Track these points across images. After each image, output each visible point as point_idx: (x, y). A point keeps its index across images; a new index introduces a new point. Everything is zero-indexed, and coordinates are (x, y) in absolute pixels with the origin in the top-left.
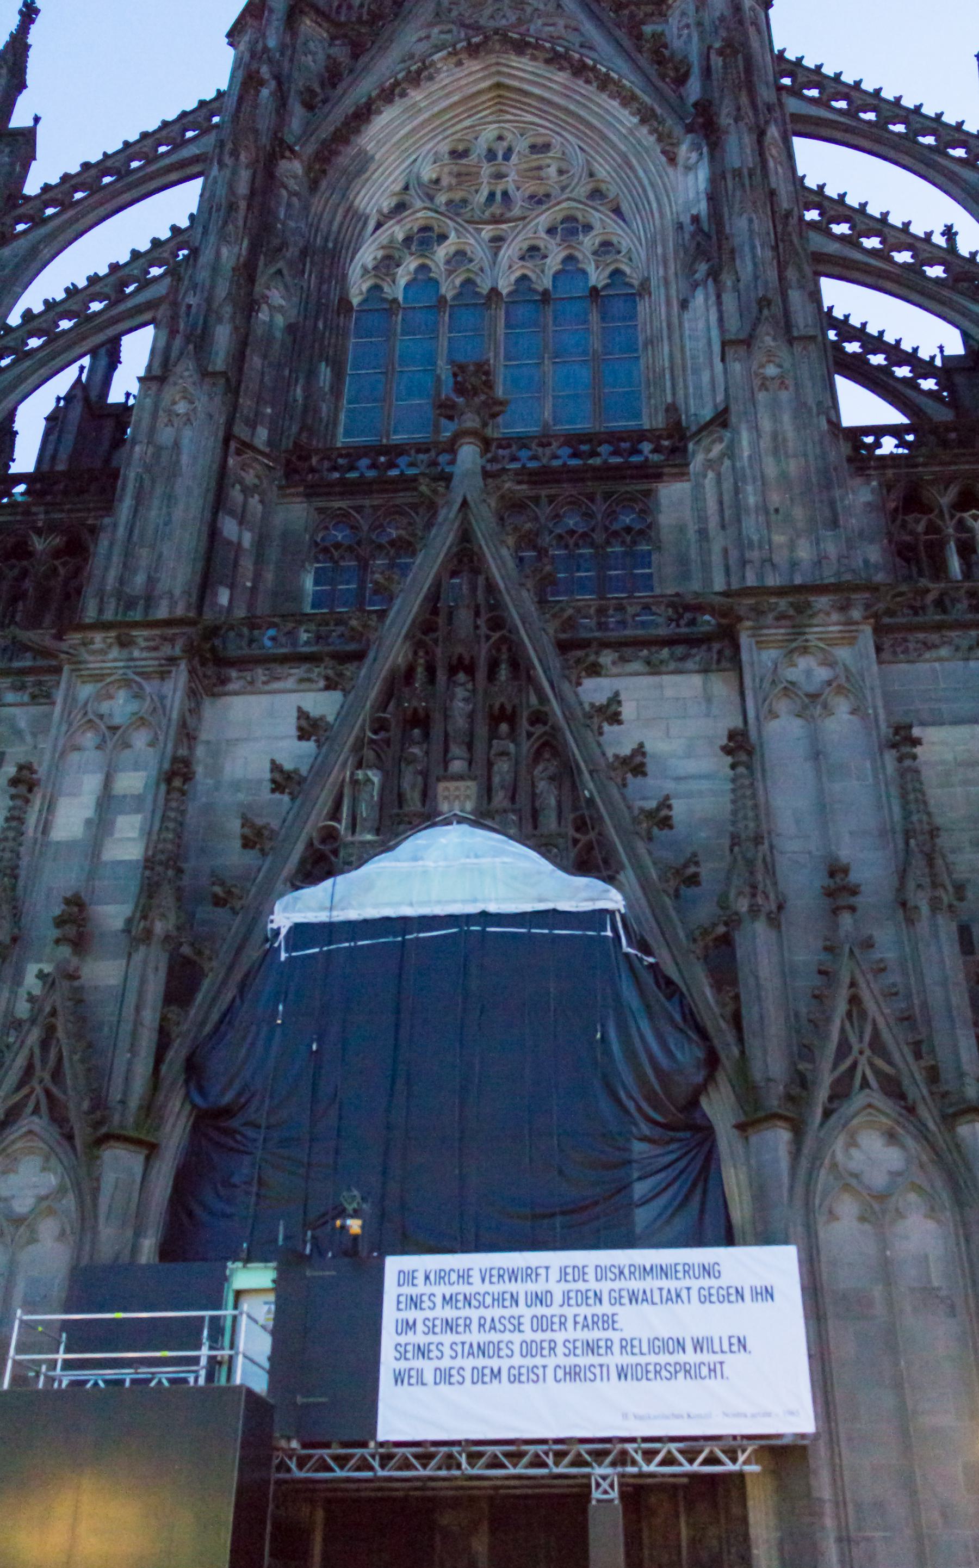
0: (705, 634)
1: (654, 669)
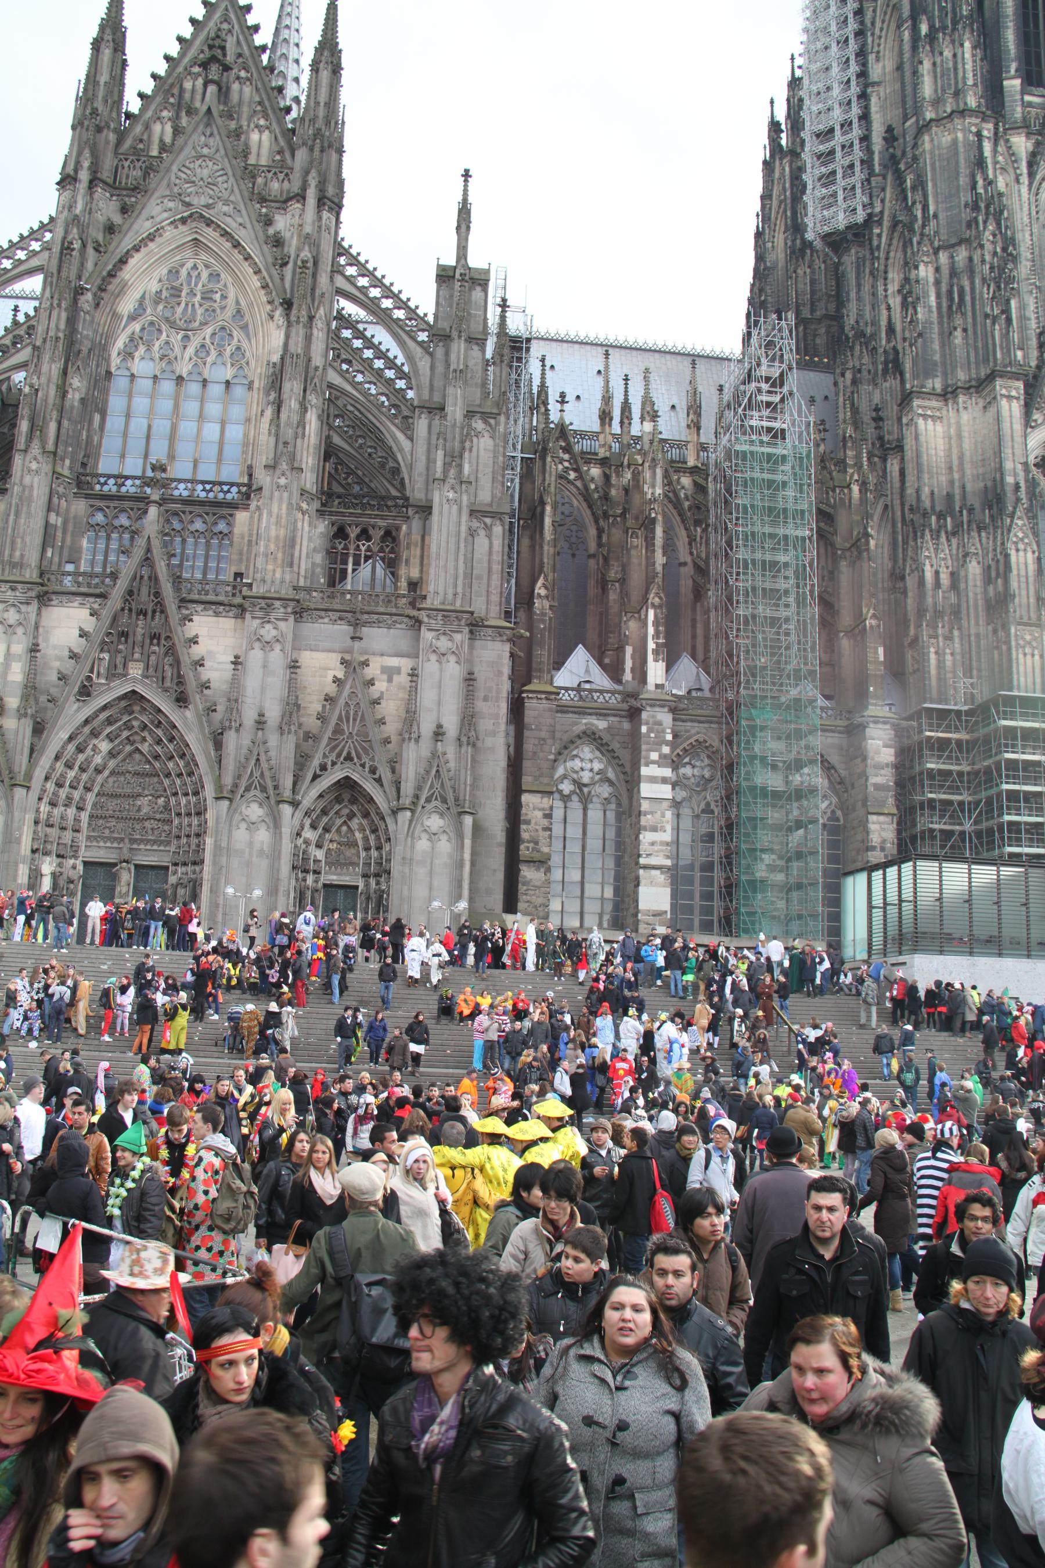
0: (239, 601)
1: (217, 614)
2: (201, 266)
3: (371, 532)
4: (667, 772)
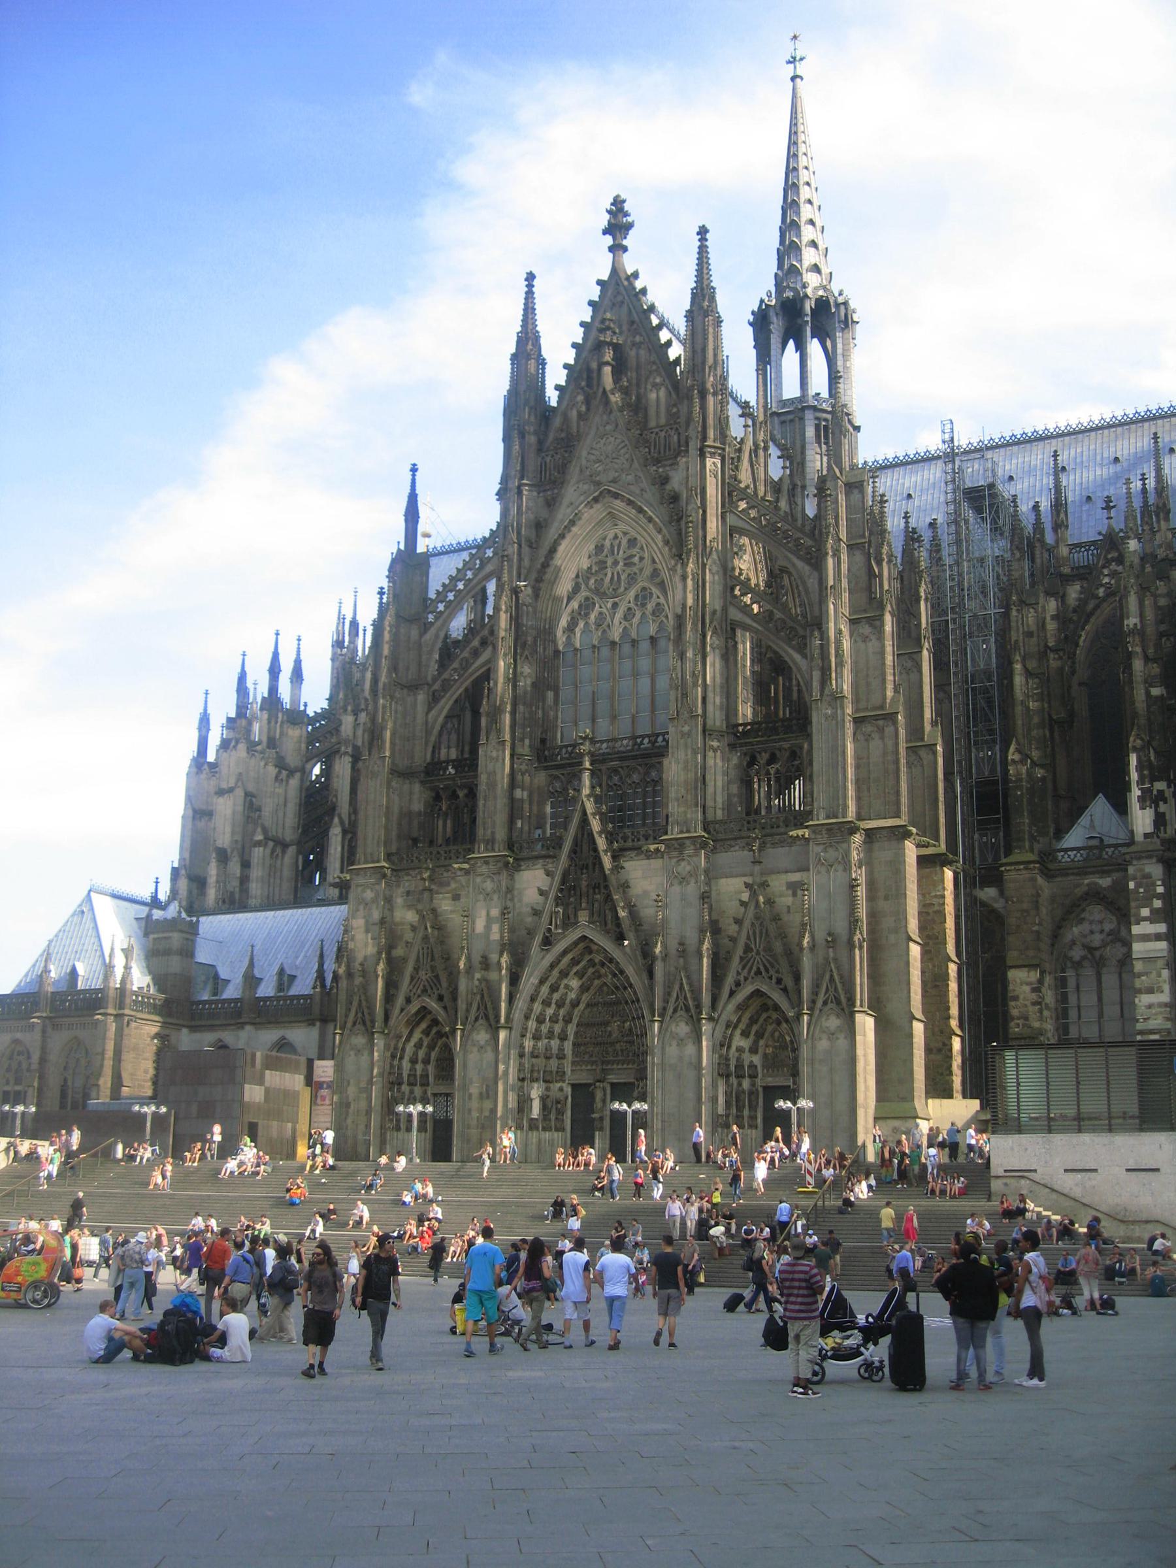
2: (620, 535)
3: (778, 753)
4: (1162, 928)
